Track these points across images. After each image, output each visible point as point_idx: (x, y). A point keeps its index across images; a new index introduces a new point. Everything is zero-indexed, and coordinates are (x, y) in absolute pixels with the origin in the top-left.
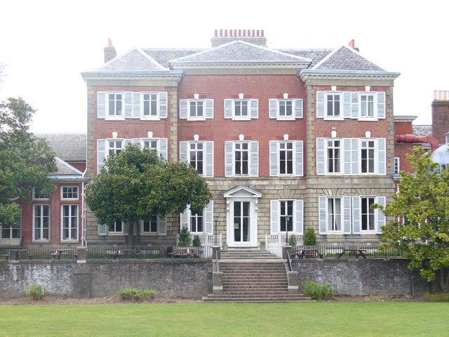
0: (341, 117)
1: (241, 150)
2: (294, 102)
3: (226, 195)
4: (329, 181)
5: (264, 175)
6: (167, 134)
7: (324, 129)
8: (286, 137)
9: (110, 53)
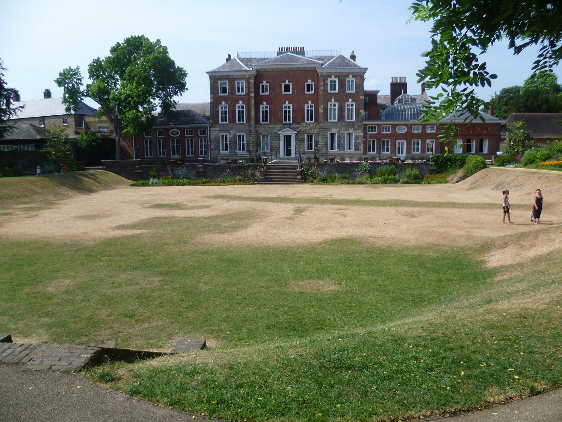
1: (287, 109)
9: (229, 59)
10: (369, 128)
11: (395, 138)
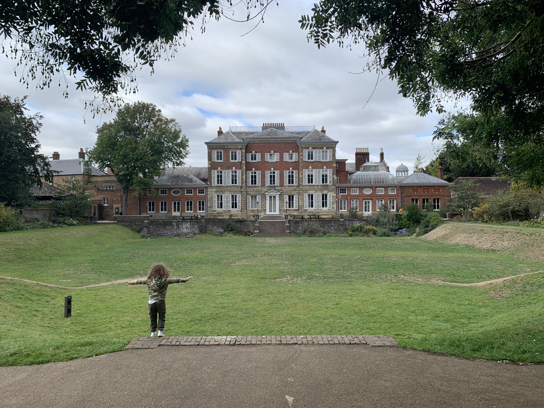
0: (314, 160)
2: (294, 154)
3: (266, 193)
4: (308, 187)
5: (282, 185)
6: (241, 168)
7: (306, 165)
8: (291, 169)
9: (220, 133)
10: (341, 190)
11: (387, 198)
